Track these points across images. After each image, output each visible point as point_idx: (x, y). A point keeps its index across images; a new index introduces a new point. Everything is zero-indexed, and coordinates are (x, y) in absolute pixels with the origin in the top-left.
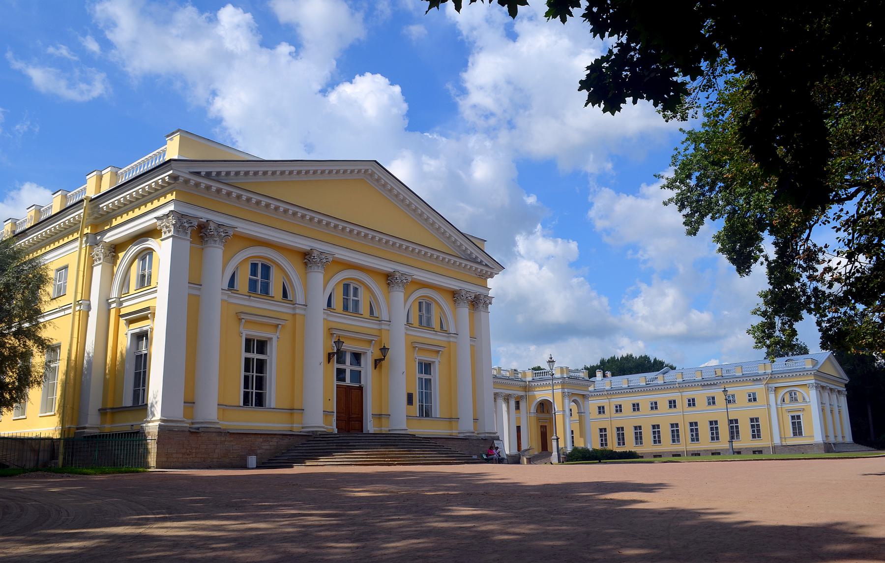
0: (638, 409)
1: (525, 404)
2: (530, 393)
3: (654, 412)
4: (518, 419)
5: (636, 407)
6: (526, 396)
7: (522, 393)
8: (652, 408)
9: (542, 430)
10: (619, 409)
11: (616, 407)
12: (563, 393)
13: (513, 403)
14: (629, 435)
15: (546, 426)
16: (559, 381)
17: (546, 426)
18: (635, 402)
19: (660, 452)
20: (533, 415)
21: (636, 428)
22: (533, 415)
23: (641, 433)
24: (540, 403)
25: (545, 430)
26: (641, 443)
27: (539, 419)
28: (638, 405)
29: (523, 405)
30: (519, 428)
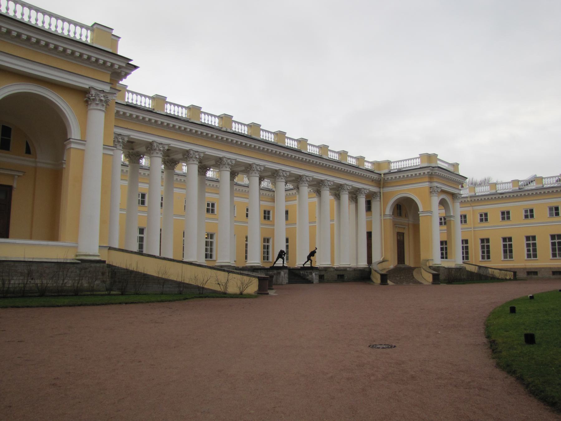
0: (508, 218)
1: (379, 203)
2: (386, 190)
3: (530, 220)
4: (369, 224)
5: (506, 215)
6: (380, 193)
7: (374, 189)
8: (526, 217)
9: (399, 238)
10: (484, 217)
11: (481, 215)
12: (431, 188)
13: (362, 201)
14: (497, 247)
15: (403, 233)
16: (426, 172)
17: (403, 233)
18: (505, 210)
19: (536, 268)
20: (389, 218)
21: (504, 239)
22: (389, 218)
23: (511, 246)
24: (397, 205)
25: (402, 238)
26: (511, 257)
27: (395, 225)
28: (508, 213)
29: (376, 205)
30: (369, 235)
